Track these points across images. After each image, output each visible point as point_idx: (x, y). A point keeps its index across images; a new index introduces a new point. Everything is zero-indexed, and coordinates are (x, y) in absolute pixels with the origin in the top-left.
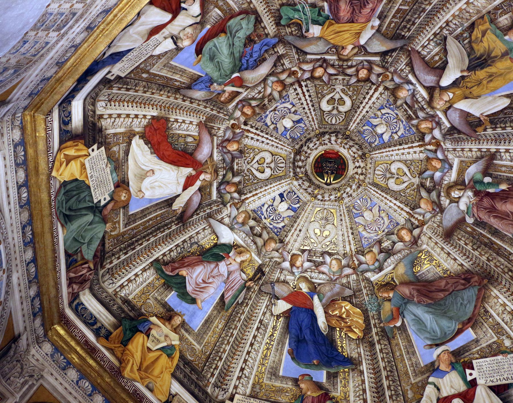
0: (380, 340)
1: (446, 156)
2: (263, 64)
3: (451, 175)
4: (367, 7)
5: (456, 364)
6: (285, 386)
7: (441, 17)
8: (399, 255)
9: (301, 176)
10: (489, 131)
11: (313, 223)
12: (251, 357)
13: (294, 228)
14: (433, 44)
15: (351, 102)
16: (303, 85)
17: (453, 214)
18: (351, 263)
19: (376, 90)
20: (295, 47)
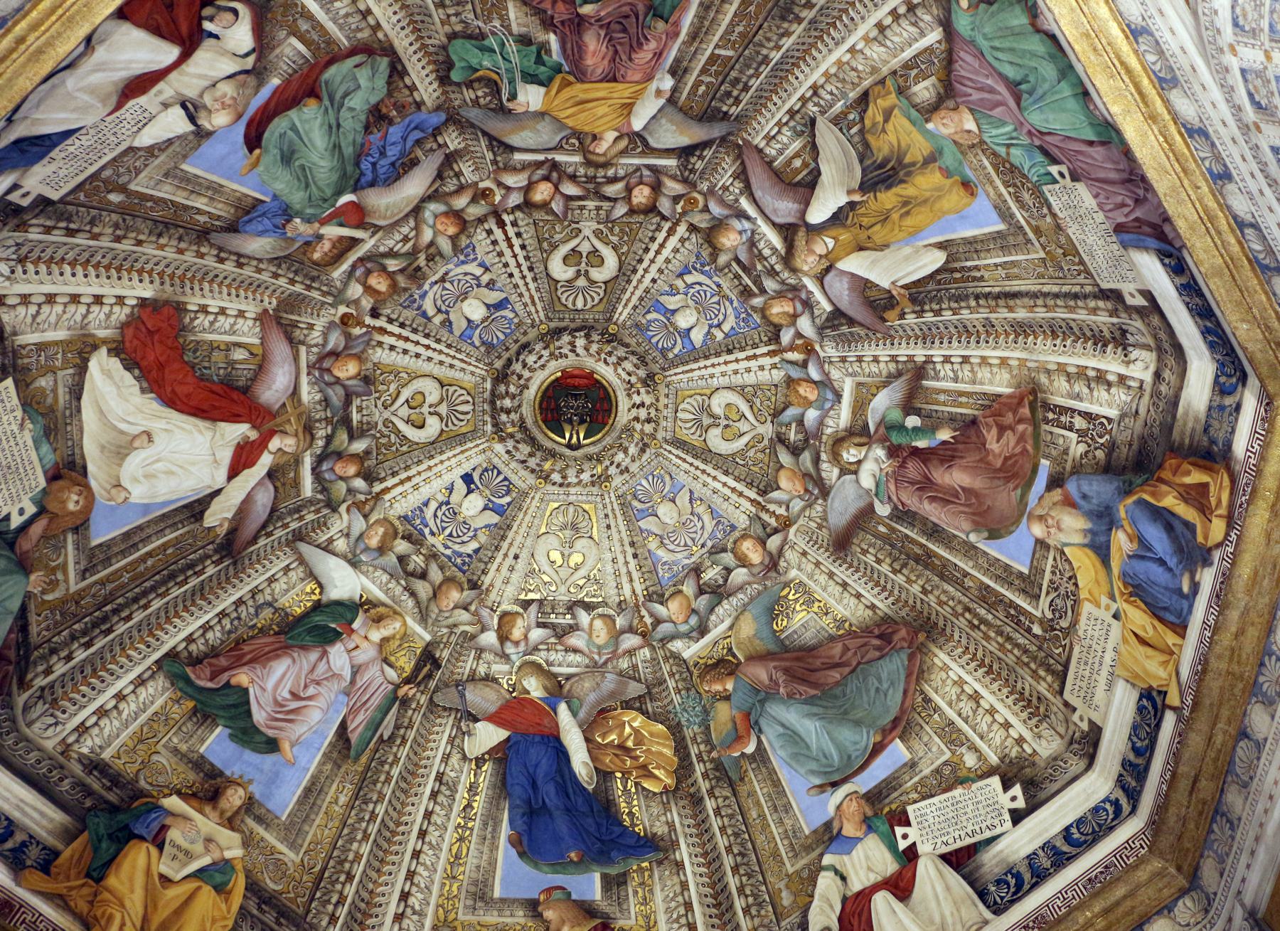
0: (712, 788)
1: (827, 375)
2: (412, 173)
3: (839, 415)
4: (645, 47)
5: (875, 820)
6: (509, 920)
7: (801, 76)
8: (741, 596)
9: (510, 430)
10: (911, 319)
11: (543, 538)
12: (424, 864)
13: (502, 552)
14: (789, 134)
15: (616, 259)
16: (508, 222)
18: (636, 622)
19: (671, 232)
20: (485, 133)
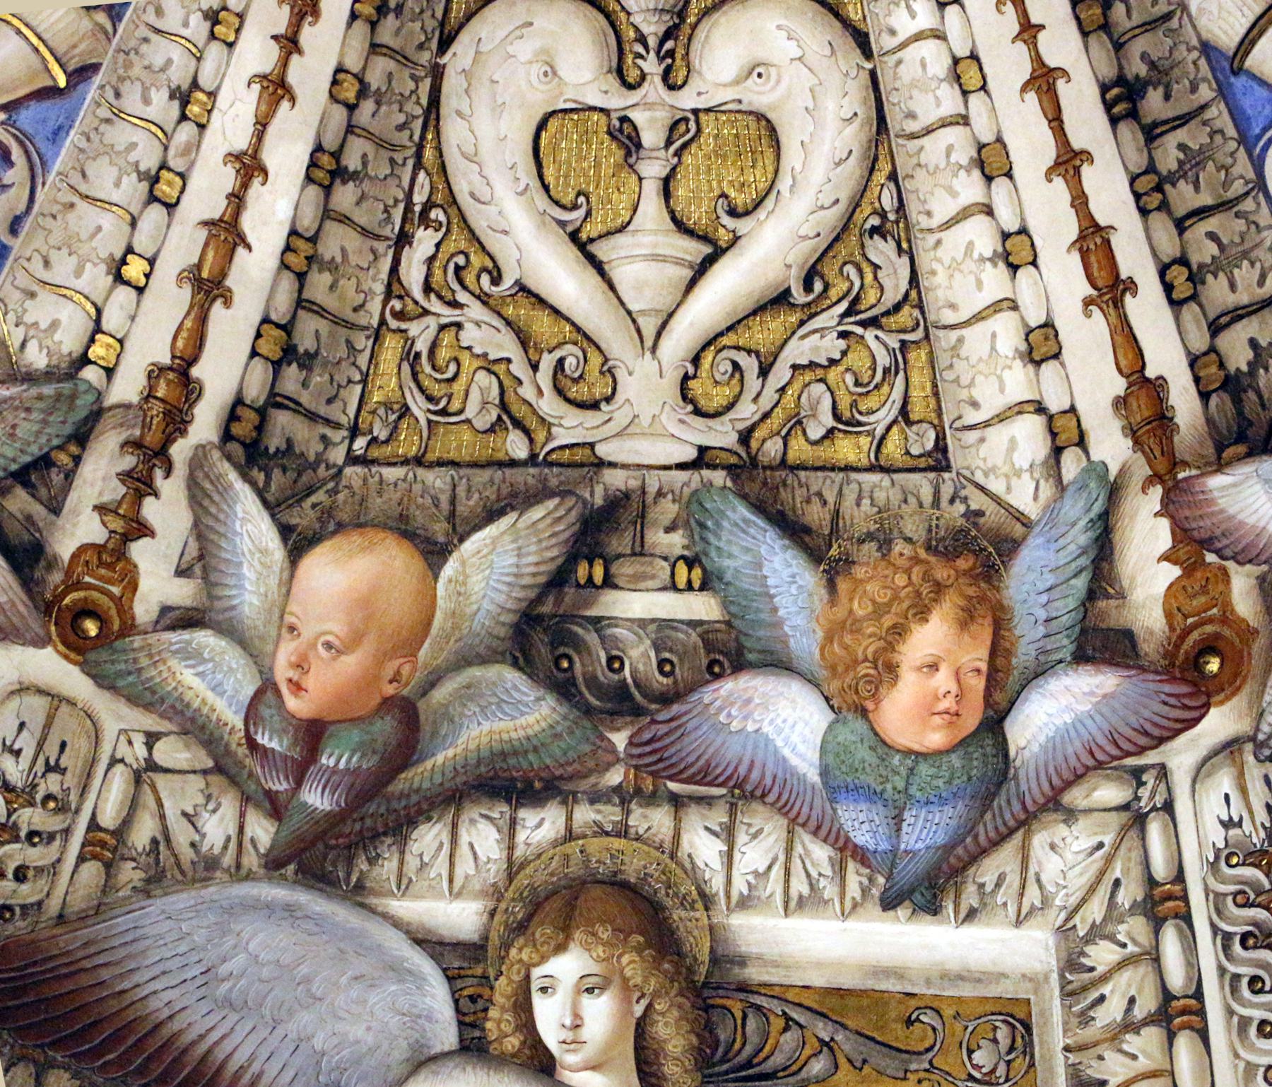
17: (305, 1019)
